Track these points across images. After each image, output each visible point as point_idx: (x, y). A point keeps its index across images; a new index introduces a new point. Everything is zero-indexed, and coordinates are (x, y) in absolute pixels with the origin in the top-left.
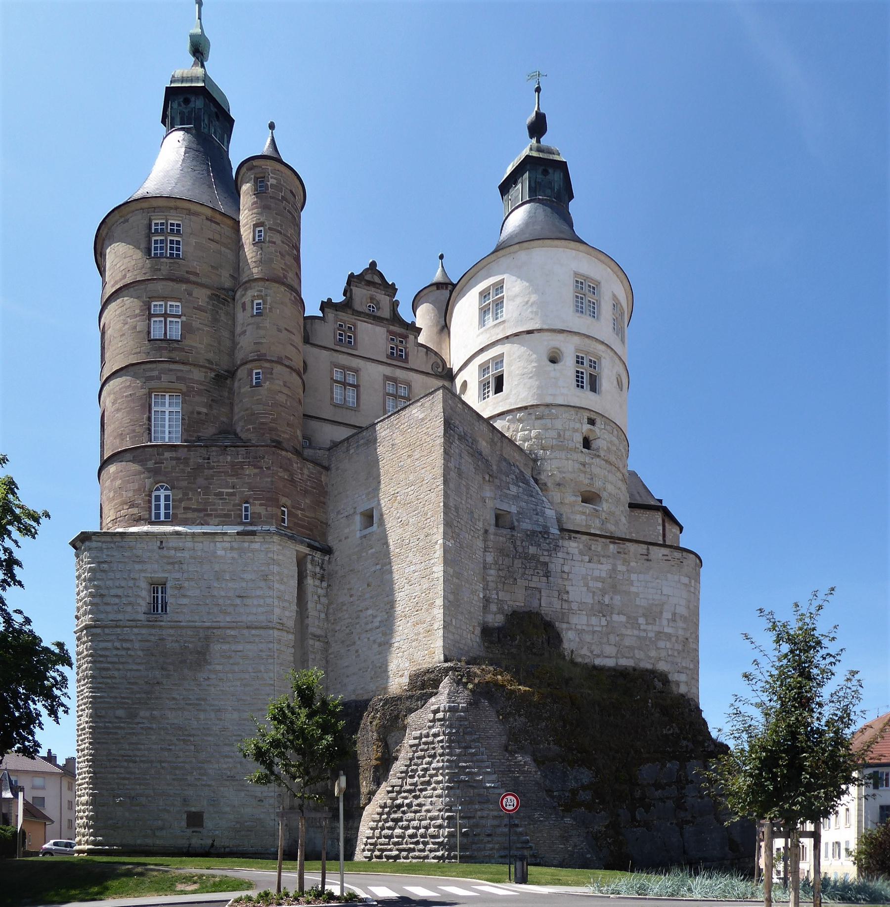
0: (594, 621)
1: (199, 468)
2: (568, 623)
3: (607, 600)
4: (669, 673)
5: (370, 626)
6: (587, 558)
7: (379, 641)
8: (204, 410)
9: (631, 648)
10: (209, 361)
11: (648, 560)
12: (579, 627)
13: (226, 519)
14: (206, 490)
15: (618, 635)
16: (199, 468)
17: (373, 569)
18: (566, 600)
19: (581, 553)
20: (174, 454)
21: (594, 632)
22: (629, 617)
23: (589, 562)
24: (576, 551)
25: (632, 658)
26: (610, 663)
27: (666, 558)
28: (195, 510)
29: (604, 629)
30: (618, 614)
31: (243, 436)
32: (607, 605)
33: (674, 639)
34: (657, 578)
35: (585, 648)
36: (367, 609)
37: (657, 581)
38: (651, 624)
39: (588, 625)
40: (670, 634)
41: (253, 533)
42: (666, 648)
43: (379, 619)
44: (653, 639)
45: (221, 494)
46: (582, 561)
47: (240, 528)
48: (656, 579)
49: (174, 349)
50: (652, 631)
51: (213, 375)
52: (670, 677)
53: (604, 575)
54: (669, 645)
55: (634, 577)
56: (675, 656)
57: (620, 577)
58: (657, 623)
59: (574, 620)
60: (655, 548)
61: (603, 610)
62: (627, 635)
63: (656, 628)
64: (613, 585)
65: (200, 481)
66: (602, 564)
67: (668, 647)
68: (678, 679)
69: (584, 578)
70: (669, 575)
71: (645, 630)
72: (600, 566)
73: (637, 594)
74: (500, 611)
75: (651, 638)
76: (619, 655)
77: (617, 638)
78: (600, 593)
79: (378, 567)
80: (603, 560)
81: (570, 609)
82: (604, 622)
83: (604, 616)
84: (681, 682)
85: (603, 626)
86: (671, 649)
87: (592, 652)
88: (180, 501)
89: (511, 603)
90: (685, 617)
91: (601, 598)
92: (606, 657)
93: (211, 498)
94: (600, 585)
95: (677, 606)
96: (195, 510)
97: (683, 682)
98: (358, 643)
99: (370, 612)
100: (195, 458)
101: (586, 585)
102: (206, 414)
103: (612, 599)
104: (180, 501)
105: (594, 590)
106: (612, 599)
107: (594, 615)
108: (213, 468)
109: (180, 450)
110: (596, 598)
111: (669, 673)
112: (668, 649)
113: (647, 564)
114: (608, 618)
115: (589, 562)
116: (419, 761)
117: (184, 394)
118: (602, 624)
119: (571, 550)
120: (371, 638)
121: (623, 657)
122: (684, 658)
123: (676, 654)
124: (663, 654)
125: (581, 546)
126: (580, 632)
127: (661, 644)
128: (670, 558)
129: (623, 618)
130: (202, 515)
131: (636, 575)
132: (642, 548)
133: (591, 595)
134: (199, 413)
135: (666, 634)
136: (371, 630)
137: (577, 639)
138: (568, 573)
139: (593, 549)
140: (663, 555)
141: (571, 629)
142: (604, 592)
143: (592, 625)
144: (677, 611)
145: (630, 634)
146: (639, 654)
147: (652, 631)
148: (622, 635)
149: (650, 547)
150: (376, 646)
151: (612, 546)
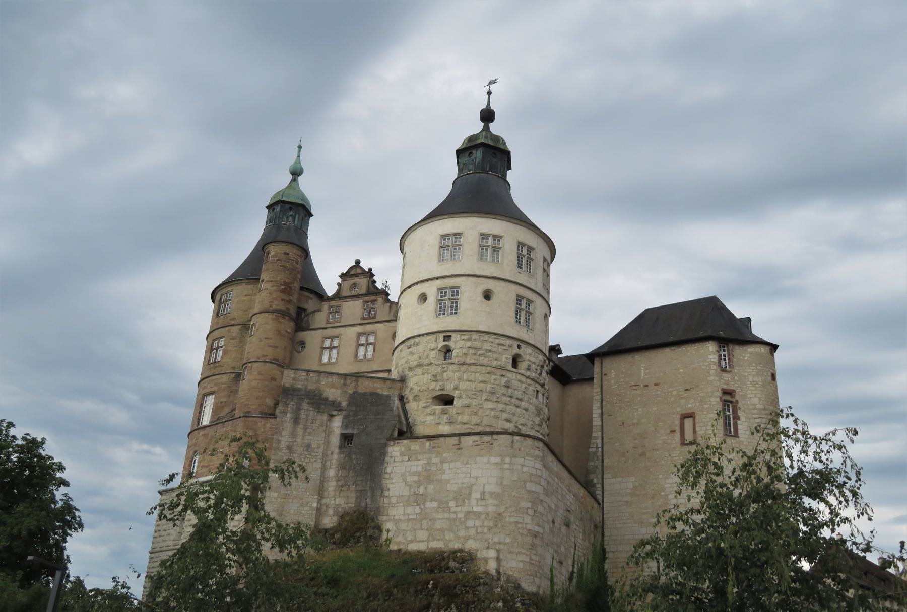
0: (410, 510)
2: (387, 515)
3: (421, 490)
4: (478, 550)
6: (406, 458)
8: (224, 400)
9: (442, 531)
10: (234, 368)
11: (459, 449)
12: (396, 518)
15: (430, 520)
18: (387, 497)
19: (402, 454)
21: (409, 520)
22: (440, 502)
23: (409, 460)
25: (442, 539)
26: (422, 547)
27: (475, 444)
29: (418, 516)
30: (431, 501)
32: (422, 495)
33: (483, 517)
34: (467, 463)
35: (401, 535)
37: (467, 466)
38: (460, 505)
39: (404, 515)
40: (479, 513)
42: (474, 526)
44: (462, 520)
46: (402, 461)
48: (466, 464)
49: (218, 367)
50: (461, 512)
52: (479, 555)
53: (420, 469)
54: (478, 523)
55: (446, 466)
56: (485, 533)
57: (434, 468)
58: (466, 504)
59: (393, 512)
60: (466, 438)
61: (418, 499)
62: (439, 519)
63: (465, 509)
64: (427, 477)
66: (419, 460)
67: (477, 525)
68: (486, 555)
69: (403, 475)
70: (478, 459)
71: (455, 512)
72: (417, 462)
73: (448, 481)
74: (336, 513)
75: (461, 519)
76: (430, 538)
77: (430, 523)
78: (416, 485)
80: (419, 456)
81: (390, 503)
82: (418, 510)
83: (418, 505)
84: (489, 558)
85: (417, 514)
86: (481, 527)
87: (406, 539)
89: (345, 506)
90: (498, 494)
91: (416, 489)
92: (419, 541)
94: (416, 478)
95: (486, 485)
97: (491, 558)
101: (405, 481)
102: (226, 402)
103: (426, 488)
105: (411, 483)
106: (426, 488)
107: (410, 505)
110: (412, 490)
111: (478, 550)
112: (477, 527)
113: (459, 452)
114: (422, 506)
115: (409, 460)
118: (416, 512)
119: (394, 454)
121: (434, 539)
122: (495, 534)
123: (486, 530)
124: (472, 532)
125: (403, 449)
126: (396, 522)
127: (470, 523)
128: (479, 443)
129: (435, 504)
131: (448, 464)
132: (454, 440)
133: (408, 488)
134: (221, 402)
135: (474, 513)
137: (394, 528)
138: (390, 473)
139: (412, 449)
140: (474, 442)
141: (389, 520)
142: (419, 483)
143: (408, 515)
144: (486, 490)
145: (441, 517)
146: (449, 536)
147: (461, 512)
148: (434, 520)
149: (462, 438)
151: (428, 444)
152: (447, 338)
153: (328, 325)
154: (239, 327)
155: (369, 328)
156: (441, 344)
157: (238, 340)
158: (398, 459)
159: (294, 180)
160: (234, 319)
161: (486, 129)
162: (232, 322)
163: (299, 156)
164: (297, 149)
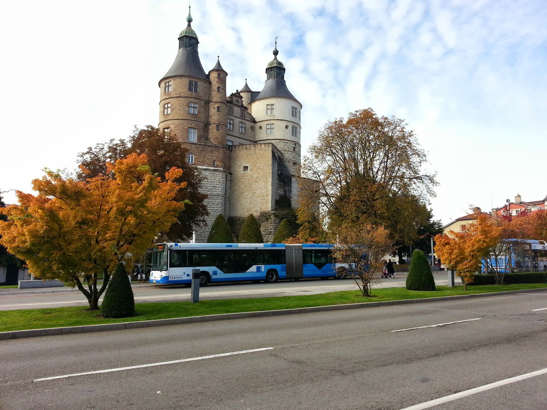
1: (202, 151)
5: (246, 197)
7: (249, 202)
8: (202, 134)
13: (209, 165)
14: (204, 157)
16: (202, 151)
17: (248, 182)
20: (195, 146)
24: (294, 181)
28: (201, 162)
31: (214, 143)
36: (245, 192)
41: (217, 170)
43: (250, 196)
45: (208, 158)
47: (213, 168)
51: (205, 124)
65: (203, 154)
69: (296, 187)
79: (250, 182)
88: (197, 159)
93: (205, 159)
96: (201, 162)
98: (242, 201)
99: (246, 193)
100: (201, 147)
104: (197, 159)
108: (206, 151)
109: (197, 145)
116: (266, 236)
117: (198, 130)
120: (247, 201)
130: (202, 163)
134: (201, 135)
136: (247, 198)
150: (248, 203)
152: (295, 144)
153: (229, 114)
154: (204, 102)
155: (243, 121)
156: (294, 146)
157: (204, 109)
158: (295, 182)
159: (189, 25)
160: (201, 97)
161: (276, 59)
162: (201, 98)
163: (190, 12)
164: (189, 8)
